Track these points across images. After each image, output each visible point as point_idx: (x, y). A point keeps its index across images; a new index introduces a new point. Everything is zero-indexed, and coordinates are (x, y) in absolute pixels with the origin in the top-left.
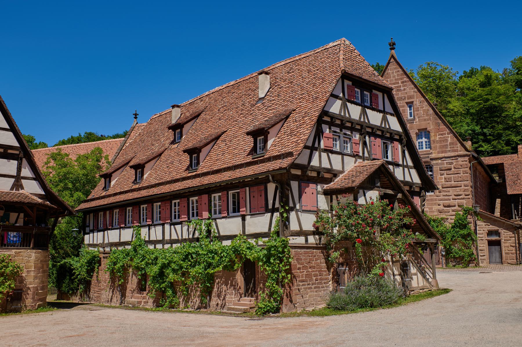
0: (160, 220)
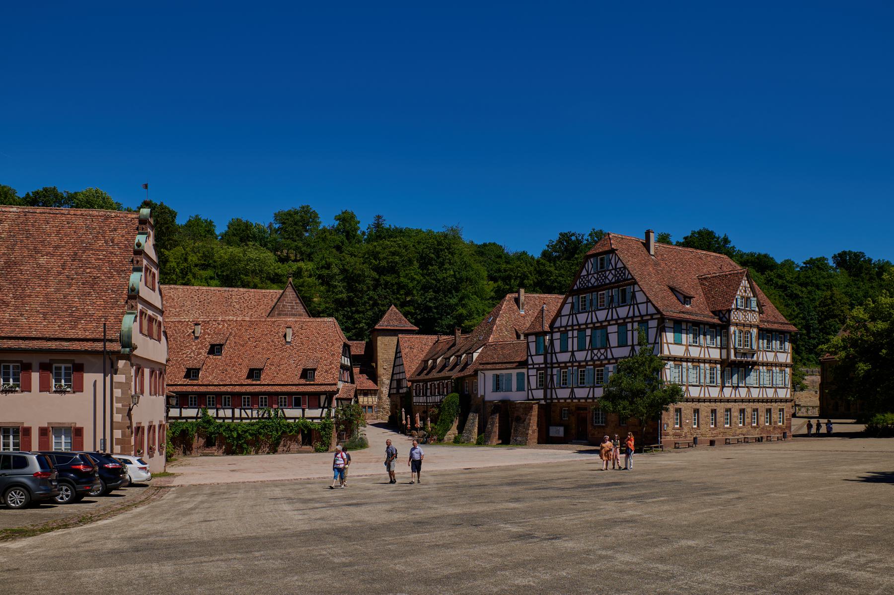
0: (229, 405)
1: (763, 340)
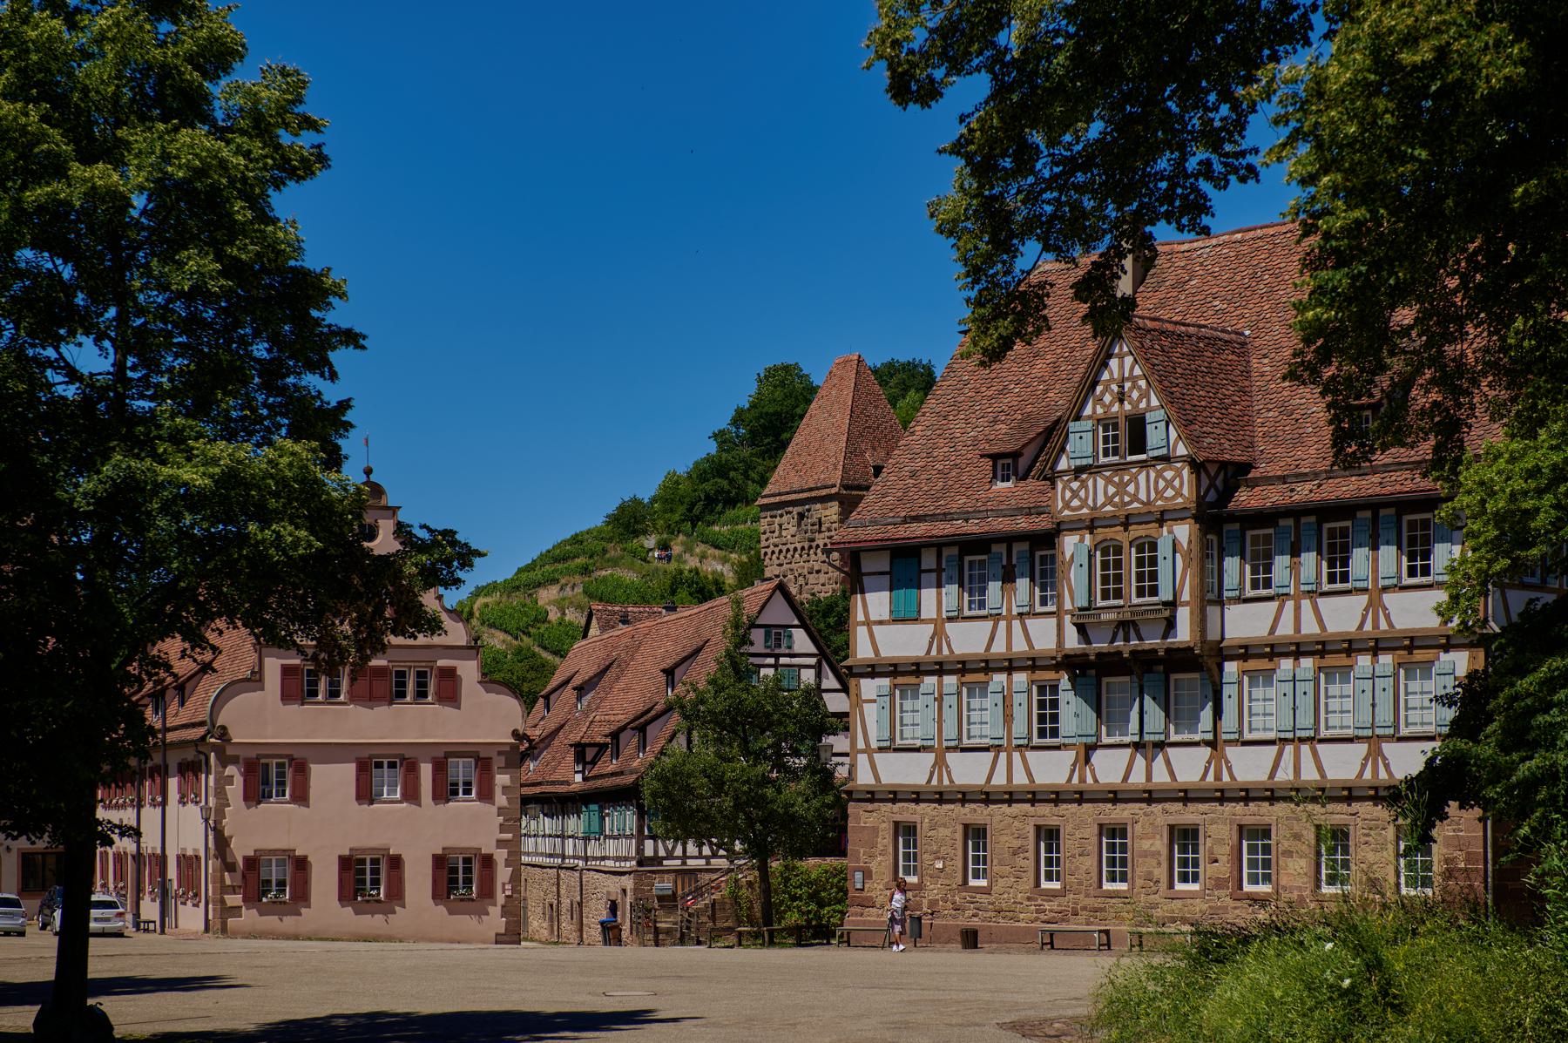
1: (1295, 552)
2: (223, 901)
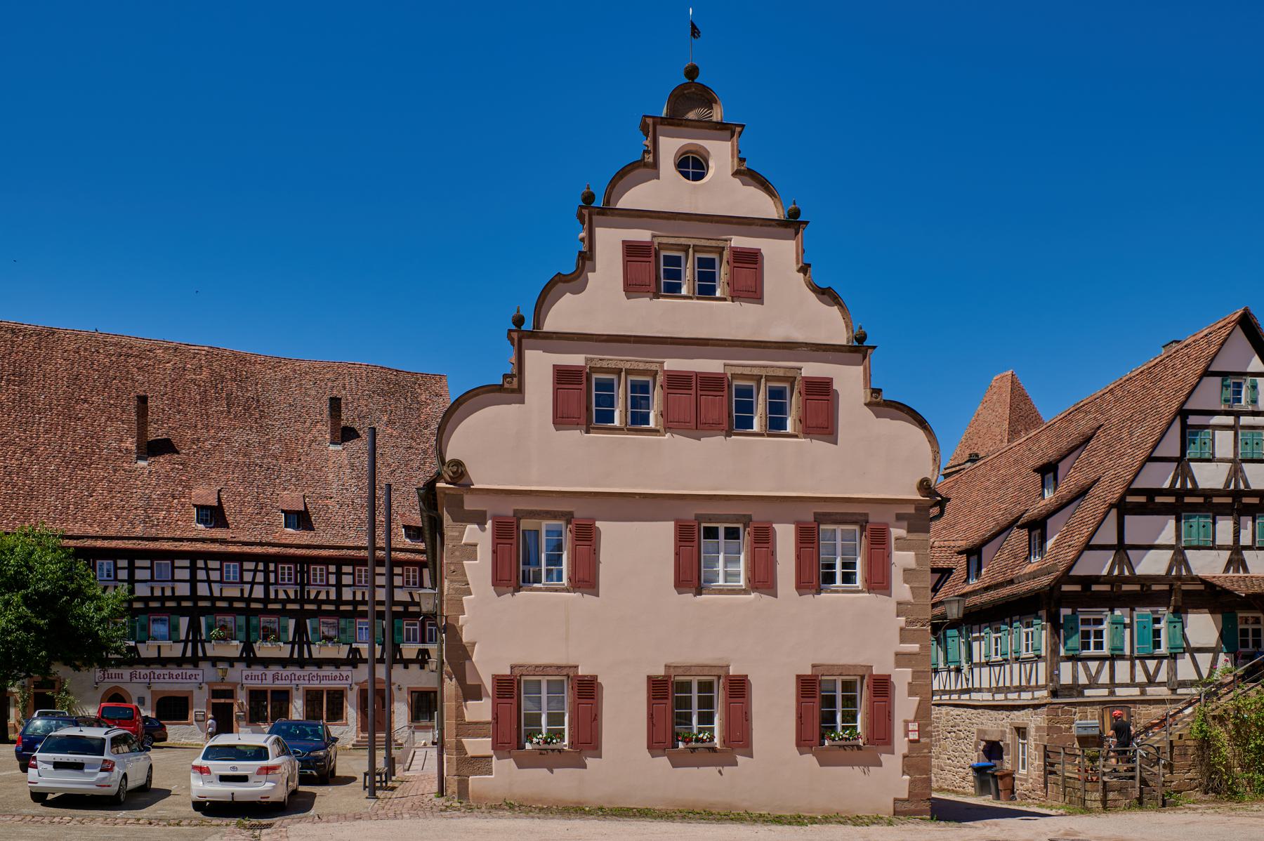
2: (460, 748)
